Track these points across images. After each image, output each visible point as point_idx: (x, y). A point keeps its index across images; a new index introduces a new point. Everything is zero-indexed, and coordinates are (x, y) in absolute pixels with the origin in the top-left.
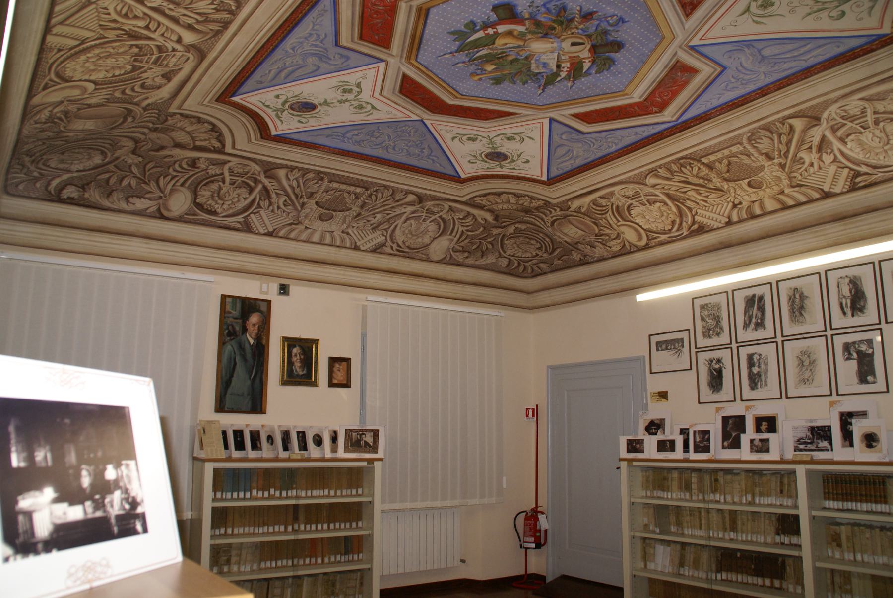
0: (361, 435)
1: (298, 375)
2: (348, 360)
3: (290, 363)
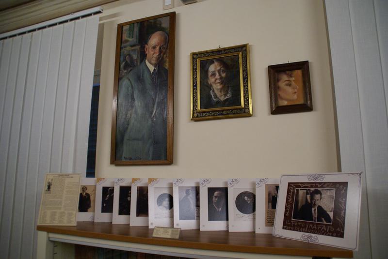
0: (313, 194)
1: (219, 103)
2: (303, 66)
3: (206, 88)
